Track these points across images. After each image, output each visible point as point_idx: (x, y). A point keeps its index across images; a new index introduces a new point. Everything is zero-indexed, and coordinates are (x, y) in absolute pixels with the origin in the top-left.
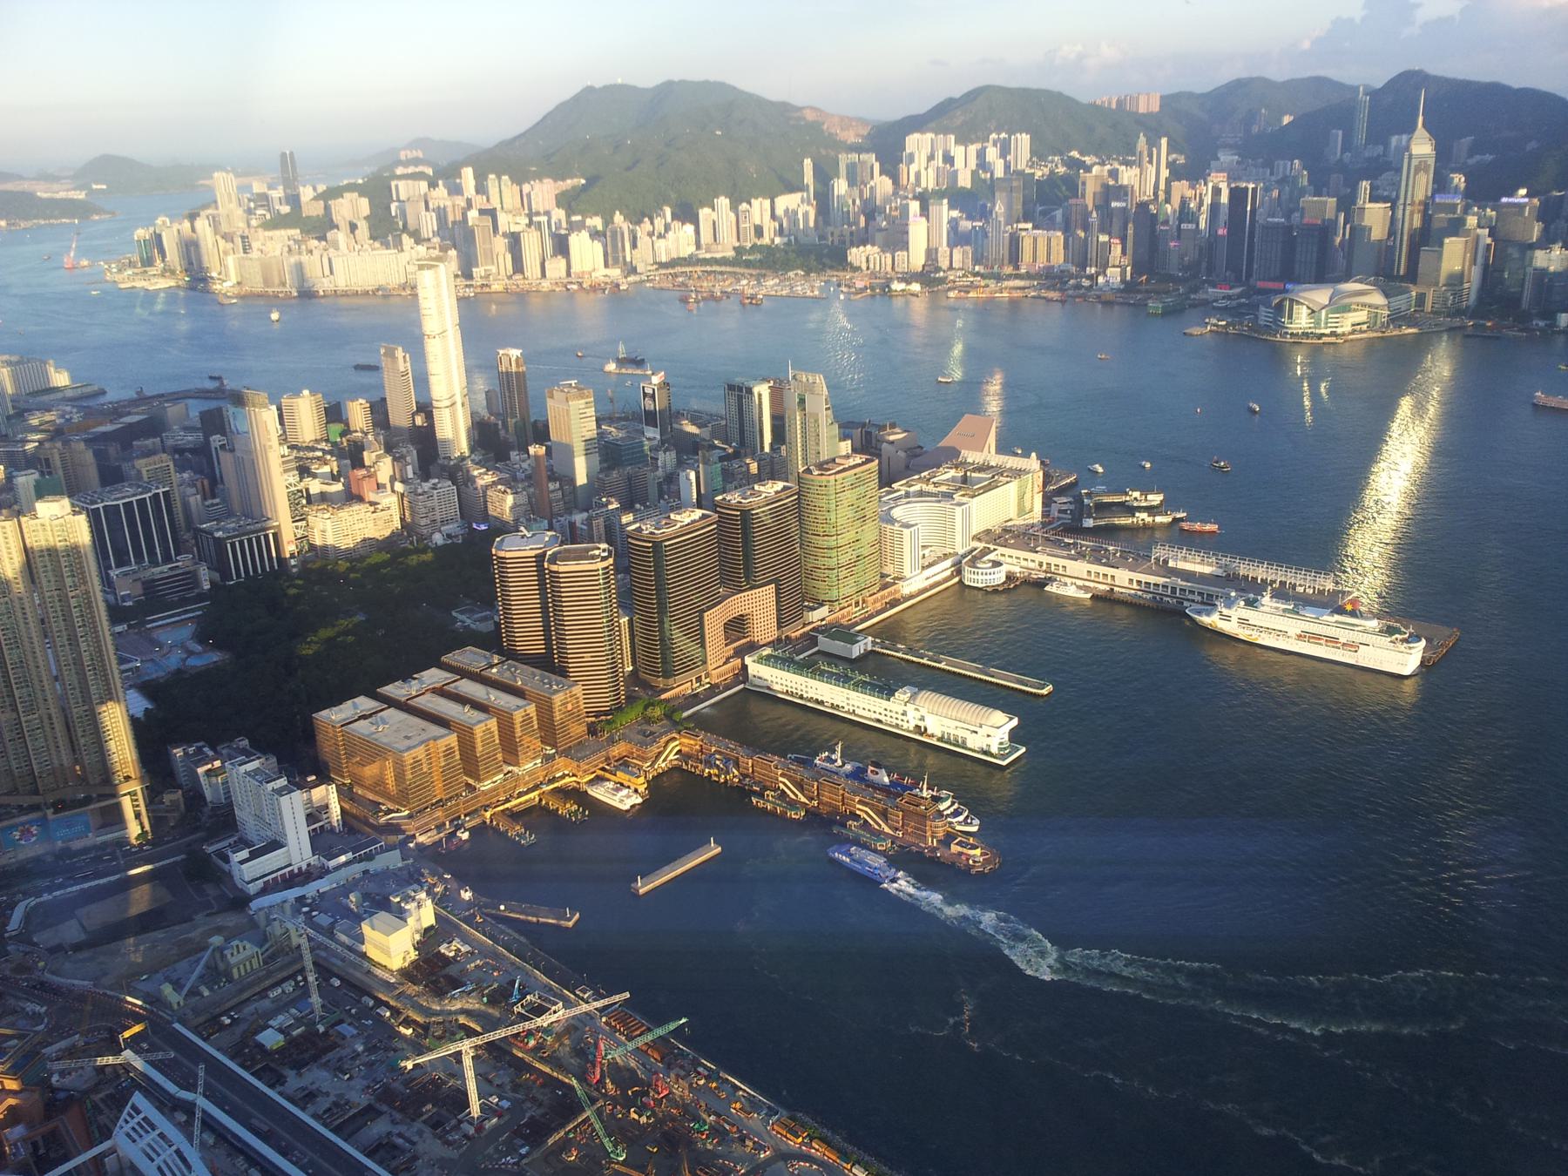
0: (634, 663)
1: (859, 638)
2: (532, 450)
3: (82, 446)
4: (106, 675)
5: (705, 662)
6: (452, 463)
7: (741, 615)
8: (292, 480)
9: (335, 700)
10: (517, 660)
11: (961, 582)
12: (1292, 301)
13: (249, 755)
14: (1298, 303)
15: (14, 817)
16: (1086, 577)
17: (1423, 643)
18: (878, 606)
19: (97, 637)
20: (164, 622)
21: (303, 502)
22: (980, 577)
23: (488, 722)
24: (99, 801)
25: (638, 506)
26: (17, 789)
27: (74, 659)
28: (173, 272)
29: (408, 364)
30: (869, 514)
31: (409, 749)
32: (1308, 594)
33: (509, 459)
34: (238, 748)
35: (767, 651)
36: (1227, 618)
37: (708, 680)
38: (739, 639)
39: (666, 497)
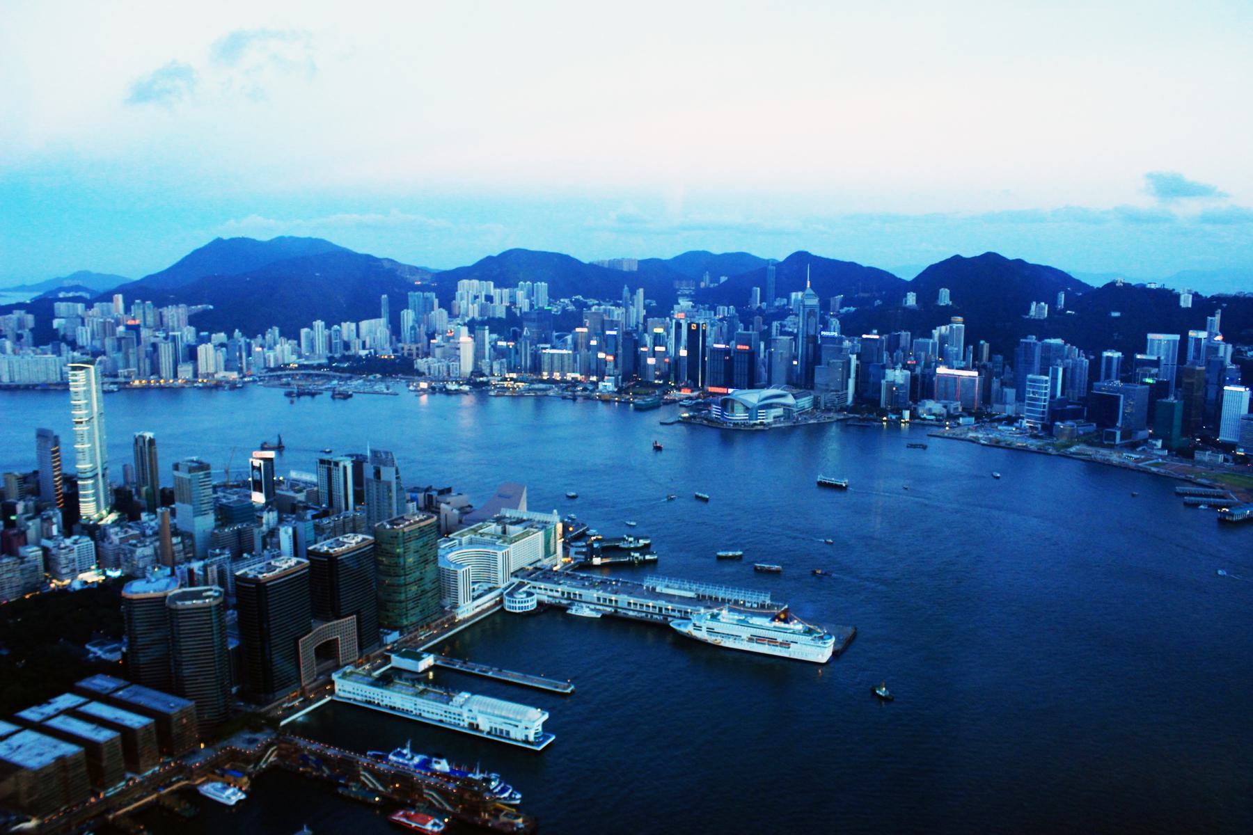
1: (424, 656)
2: (159, 510)
6: (91, 522)
7: (330, 641)
11: (503, 609)
12: (733, 401)
16: (596, 601)
17: (834, 639)
22: (518, 605)
25: (245, 555)
32: (754, 608)
33: (140, 519)
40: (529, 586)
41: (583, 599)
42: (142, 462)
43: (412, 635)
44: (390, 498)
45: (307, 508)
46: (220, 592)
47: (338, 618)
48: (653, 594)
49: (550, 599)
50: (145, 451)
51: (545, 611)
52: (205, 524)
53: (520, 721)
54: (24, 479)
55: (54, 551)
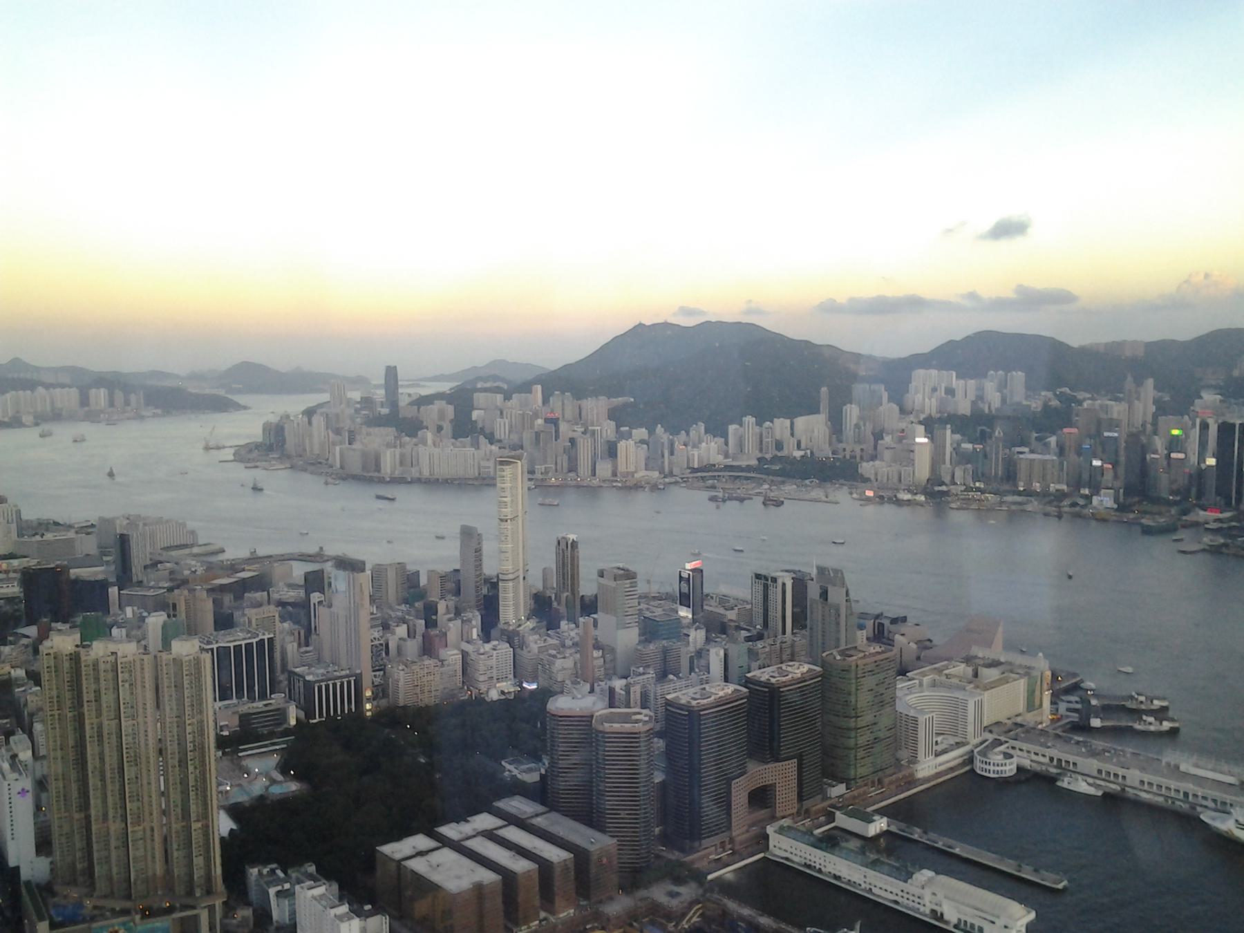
1: (874, 818)
4: (205, 797)
5: (729, 828)
6: (511, 628)
8: (376, 635)
9: (398, 838)
10: (555, 811)
11: (973, 771)
15: (106, 919)
16: (1095, 773)
22: (992, 768)
24: (181, 911)
25: (671, 677)
26: (112, 892)
28: (289, 457)
37: (730, 846)
39: (697, 670)
40: (1006, 745)
41: (1078, 771)
43: (861, 790)
44: (838, 624)
45: (738, 628)
46: (650, 717)
47: (778, 760)
49: (1033, 764)
50: (567, 553)
51: (1027, 780)
52: (627, 638)
53: (998, 917)
54: (444, 578)
55: (473, 656)
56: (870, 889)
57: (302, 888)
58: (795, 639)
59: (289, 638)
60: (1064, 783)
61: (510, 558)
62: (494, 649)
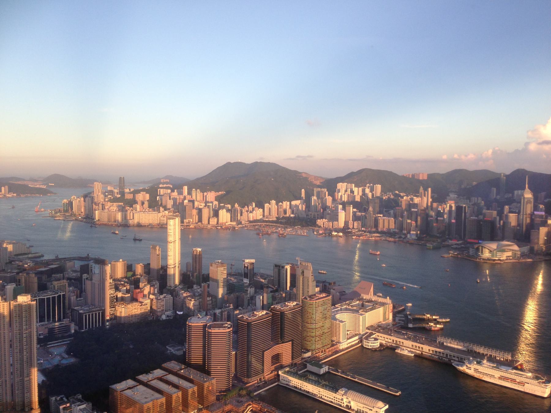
0: (236, 370)
1: (323, 366)
2: (202, 284)
3: (34, 275)
5: (263, 372)
6: (172, 288)
8: (112, 292)
9: (120, 381)
10: (190, 367)
11: (362, 346)
12: (482, 247)
13: (81, 401)
14: (485, 248)
16: (411, 347)
18: (330, 353)
19: (31, 350)
20: (54, 345)
21: (116, 300)
23: (178, 393)
27: (20, 358)
29: (160, 252)
30: (328, 316)
31: (146, 402)
32: (501, 361)
33: (193, 287)
34: (77, 398)
35: (287, 369)
36: (470, 368)
38: (277, 363)
39: (251, 305)
40: (376, 335)
41: (404, 345)
42: (195, 261)
45: (268, 287)
47: (283, 343)
48: (442, 346)
56: (321, 397)
57: (75, 406)
58: (291, 291)
59: (72, 294)
60: (398, 351)
61: (172, 259)
62: (164, 298)
